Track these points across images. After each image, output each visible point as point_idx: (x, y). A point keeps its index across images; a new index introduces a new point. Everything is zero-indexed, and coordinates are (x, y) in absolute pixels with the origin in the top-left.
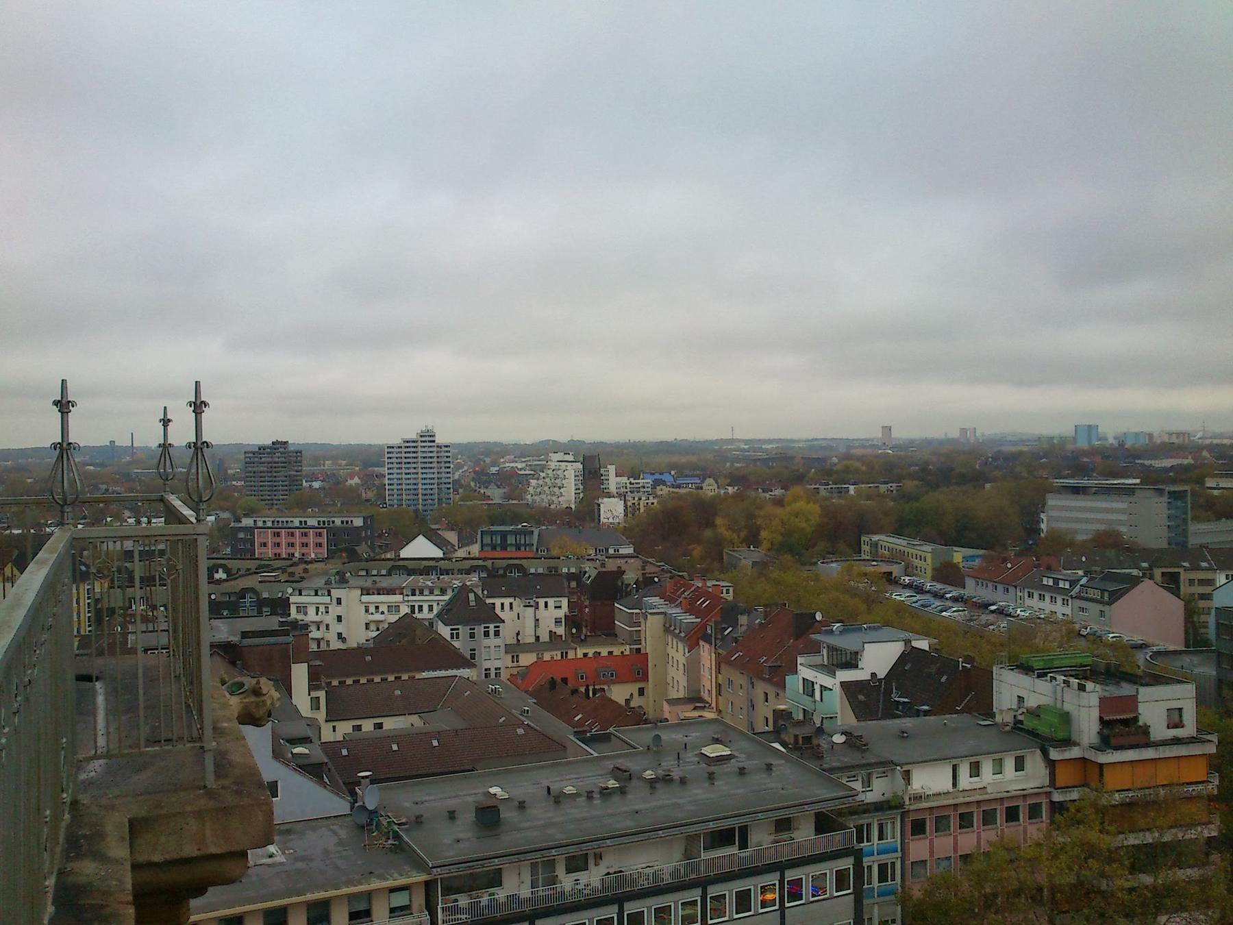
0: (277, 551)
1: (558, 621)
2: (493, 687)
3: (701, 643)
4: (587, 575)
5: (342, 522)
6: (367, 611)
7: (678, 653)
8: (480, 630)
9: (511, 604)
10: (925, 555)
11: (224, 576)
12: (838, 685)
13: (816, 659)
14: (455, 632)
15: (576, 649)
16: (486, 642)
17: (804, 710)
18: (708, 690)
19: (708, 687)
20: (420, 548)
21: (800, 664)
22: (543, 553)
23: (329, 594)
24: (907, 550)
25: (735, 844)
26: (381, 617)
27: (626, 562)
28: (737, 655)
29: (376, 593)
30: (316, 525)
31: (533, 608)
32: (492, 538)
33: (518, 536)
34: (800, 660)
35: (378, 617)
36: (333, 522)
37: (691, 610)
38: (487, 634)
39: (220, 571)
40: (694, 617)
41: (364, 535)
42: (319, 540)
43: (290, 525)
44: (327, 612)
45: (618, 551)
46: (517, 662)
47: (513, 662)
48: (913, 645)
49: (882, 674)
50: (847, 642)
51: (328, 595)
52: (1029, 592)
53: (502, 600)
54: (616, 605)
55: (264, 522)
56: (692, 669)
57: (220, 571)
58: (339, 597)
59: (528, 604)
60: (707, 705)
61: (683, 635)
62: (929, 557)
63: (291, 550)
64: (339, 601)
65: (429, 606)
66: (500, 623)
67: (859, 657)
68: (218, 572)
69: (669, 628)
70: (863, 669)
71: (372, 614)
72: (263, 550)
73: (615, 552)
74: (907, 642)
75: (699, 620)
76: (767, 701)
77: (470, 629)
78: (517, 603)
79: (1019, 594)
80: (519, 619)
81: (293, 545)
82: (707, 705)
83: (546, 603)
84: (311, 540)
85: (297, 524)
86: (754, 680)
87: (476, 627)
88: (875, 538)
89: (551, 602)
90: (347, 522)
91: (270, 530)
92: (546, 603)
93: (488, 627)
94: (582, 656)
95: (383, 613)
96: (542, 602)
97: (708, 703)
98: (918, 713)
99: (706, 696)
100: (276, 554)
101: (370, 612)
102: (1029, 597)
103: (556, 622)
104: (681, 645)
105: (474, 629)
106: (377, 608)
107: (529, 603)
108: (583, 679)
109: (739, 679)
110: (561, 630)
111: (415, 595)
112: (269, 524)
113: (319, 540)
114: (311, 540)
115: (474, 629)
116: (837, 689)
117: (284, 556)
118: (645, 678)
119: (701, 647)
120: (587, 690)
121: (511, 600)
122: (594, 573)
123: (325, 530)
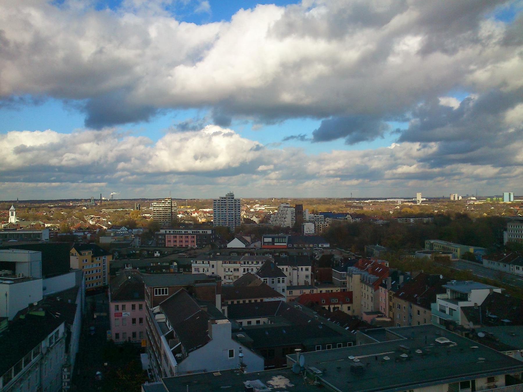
0: (175, 244)
1: (307, 277)
2: (297, 306)
3: (380, 288)
4: (317, 256)
5: (203, 232)
6: (225, 269)
7: (369, 291)
8: (276, 280)
9: (287, 268)
10: (459, 250)
11: (159, 255)
12: (460, 309)
13: (444, 296)
14: (265, 280)
15: (317, 289)
16: (279, 285)
17: (440, 318)
18: (384, 309)
19: (384, 307)
20: (236, 243)
21: (438, 298)
22: (290, 246)
23: (209, 263)
24: (447, 246)
25: (470, 387)
26: (231, 273)
27: (332, 251)
28: (402, 294)
29: (229, 263)
30: (192, 233)
31: (297, 270)
32: (278, 239)
33: (279, 239)
34: (438, 296)
35: (229, 273)
36: (199, 232)
37: (373, 272)
38: (279, 282)
39: (157, 252)
40: (375, 276)
41: (212, 237)
42: (193, 240)
43: (180, 233)
44: (208, 271)
45: (323, 246)
46: (292, 294)
47: (290, 294)
48: (494, 291)
49: (479, 304)
50: (461, 288)
51: (208, 264)
52: (517, 267)
53: (302, 267)
54: (333, 270)
55: (170, 231)
56: (375, 299)
57: (157, 252)
58: (213, 264)
59: (294, 269)
60: (383, 315)
61: (371, 284)
62: (459, 250)
63: (187, 244)
64: (213, 266)
65: (244, 269)
66: (285, 277)
67: (469, 296)
68: (156, 253)
69: (363, 281)
70: (470, 301)
71: (227, 272)
72: (169, 243)
73: (322, 246)
74: (491, 290)
75: (378, 277)
76: (419, 315)
77: (272, 279)
78: (290, 268)
79: (511, 267)
80: (290, 275)
81: (182, 241)
82: (383, 315)
83: (302, 268)
84: (190, 239)
85: (183, 233)
86: (412, 305)
87: (274, 278)
88: (432, 242)
89: (304, 268)
90: (205, 232)
91: (172, 235)
92: (302, 268)
93: (280, 279)
94: (320, 293)
95: (231, 272)
96: (300, 267)
97: (384, 314)
98: (503, 324)
99: (383, 311)
100: (175, 245)
101: (226, 271)
102: (517, 269)
103: (306, 277)
104: (370, 289)
105: (274, 279)
106: (229, 269)
107: (295, 268)
108: (323, 301)
109: (404, 304)
110: (309, 280)
111: (245, 264)
112: (172, 232)
113: (193, 240)
114: (190, 239)
115: (274, 279)
116: (459, 310)
117: (184, 246)
118: (351, 302)
119: (380, 289)
120: (329, 308)
121: (287, 267)
122: (321, 255)
123: (196, 235)
